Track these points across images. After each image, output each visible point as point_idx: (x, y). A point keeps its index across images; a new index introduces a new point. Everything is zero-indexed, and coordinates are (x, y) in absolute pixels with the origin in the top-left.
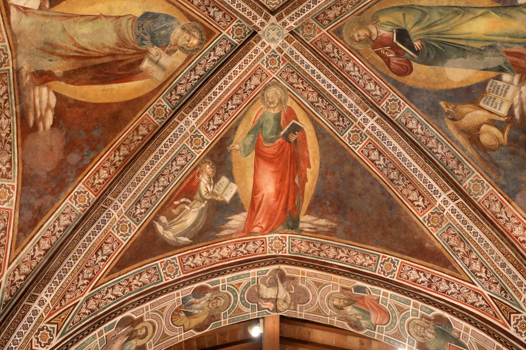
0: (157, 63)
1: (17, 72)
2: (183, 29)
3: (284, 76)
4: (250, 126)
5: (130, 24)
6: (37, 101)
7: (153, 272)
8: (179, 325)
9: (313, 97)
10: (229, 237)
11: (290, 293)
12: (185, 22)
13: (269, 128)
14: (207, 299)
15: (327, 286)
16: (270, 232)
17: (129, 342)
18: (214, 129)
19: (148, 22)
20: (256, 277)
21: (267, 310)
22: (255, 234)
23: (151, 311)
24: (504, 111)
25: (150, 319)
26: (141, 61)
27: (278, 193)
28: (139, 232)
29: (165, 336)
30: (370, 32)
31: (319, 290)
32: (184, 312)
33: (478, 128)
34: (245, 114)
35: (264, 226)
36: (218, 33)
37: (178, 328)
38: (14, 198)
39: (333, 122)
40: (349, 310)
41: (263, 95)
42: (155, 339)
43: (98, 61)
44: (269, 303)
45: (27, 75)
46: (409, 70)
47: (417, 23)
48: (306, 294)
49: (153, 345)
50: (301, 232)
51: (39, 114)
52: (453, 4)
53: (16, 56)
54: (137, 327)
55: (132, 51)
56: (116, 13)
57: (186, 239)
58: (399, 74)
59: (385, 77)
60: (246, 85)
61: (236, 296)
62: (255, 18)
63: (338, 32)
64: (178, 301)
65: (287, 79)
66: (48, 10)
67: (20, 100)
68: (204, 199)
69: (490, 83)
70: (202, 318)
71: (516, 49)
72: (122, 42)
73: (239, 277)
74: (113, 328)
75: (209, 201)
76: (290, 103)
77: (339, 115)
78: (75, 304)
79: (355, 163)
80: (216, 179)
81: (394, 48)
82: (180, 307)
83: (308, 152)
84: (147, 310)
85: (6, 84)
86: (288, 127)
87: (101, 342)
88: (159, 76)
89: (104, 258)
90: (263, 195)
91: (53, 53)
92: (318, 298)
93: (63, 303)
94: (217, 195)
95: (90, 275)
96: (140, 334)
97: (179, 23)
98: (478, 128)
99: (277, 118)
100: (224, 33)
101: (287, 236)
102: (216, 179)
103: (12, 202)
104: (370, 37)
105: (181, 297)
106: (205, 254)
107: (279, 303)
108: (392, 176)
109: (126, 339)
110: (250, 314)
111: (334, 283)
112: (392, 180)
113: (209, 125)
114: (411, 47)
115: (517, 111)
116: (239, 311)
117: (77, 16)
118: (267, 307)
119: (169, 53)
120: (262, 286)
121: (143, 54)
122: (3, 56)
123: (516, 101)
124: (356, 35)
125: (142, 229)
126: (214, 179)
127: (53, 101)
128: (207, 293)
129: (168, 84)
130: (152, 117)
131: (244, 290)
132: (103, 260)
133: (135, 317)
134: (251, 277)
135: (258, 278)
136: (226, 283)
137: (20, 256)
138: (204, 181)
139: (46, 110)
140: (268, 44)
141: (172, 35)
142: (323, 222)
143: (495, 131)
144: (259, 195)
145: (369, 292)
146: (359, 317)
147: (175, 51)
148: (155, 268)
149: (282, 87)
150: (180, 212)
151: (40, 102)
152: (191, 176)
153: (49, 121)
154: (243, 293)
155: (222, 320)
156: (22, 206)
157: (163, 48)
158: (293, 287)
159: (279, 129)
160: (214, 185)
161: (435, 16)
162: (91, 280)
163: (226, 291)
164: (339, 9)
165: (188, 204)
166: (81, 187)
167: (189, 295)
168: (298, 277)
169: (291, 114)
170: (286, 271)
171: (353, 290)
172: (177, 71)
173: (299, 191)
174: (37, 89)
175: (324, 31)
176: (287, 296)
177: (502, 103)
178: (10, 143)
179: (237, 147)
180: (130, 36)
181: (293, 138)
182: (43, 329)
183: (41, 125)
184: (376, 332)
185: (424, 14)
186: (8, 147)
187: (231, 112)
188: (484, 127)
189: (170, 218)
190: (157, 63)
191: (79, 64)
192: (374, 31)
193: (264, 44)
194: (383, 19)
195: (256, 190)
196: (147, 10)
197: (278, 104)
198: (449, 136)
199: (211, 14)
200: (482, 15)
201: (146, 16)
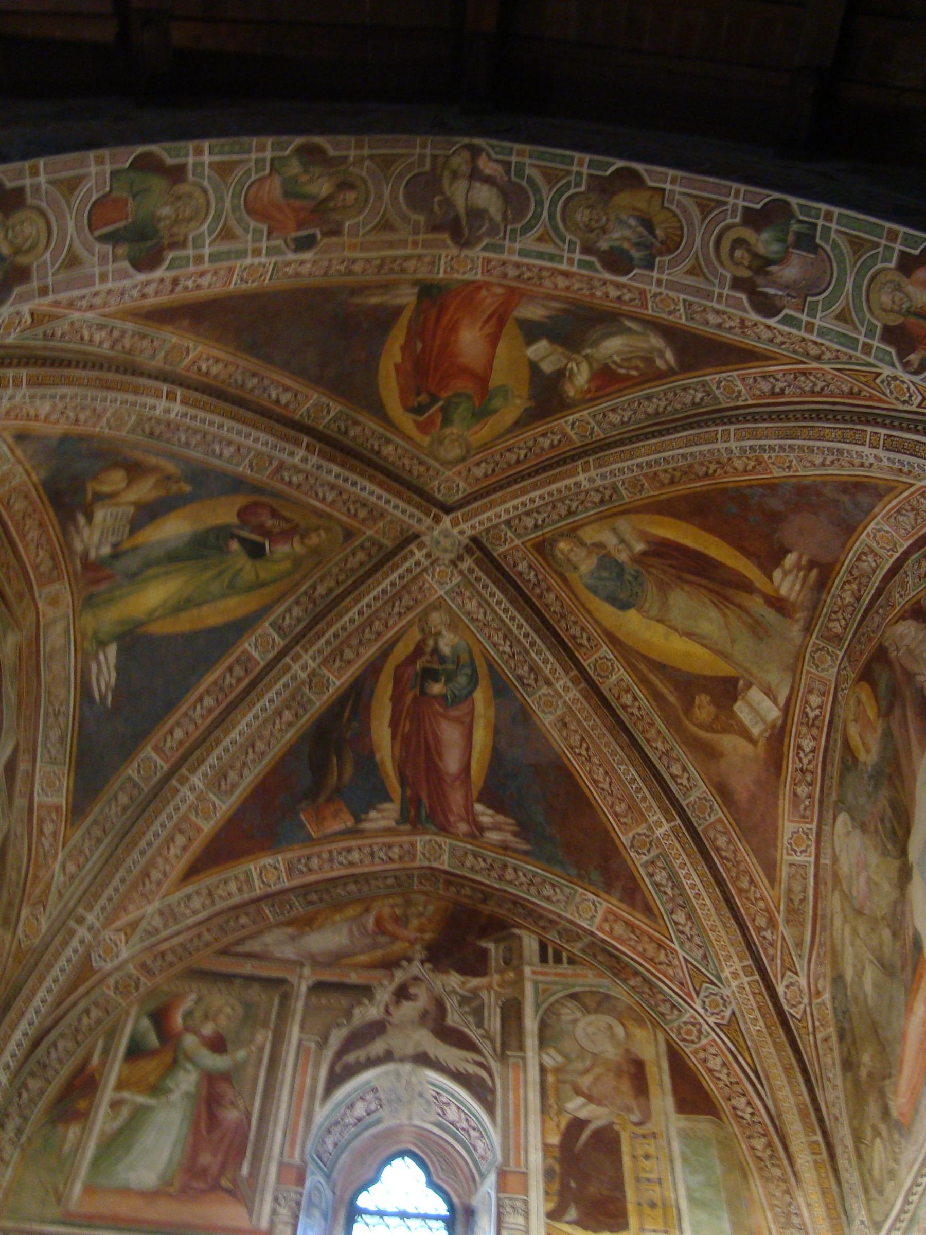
0: (622, 541)
1: (808, 630)
2: (576, 568)
3: (431, 472)
4: (492, 420)
5: (647, 605)
6: (797, 587)
7: (697, 317)
8: (670, 215)
9: (388, 450)
10: (548, 297)
11: (443, 193)
12: (572, 576)
13: (461, 411)
14: (606, 237)
15: (369, 227)
16: (473, 282)
17: (771, 256)
18: (553, 433)
19: (623, 596)
20: (507, 243)
21: (494, 156)
22: (500, 285)
23: (714, 285)
24: (100, 515)
25: (720, 270)
26: (644, 554)
27: (454, 328)
28: (707, 371)
29: (705, 207)
30: (302, 542)
31: (384, 215)
32: (655, 237)
33: (130, 483)
34: (500, 437)
35: (484, 292)
36: (528, 544)
37: (674, 208)
38: (872, 525)
39: (356, 423)
40: (323, 188)
41: (468, 451)
42: (721, 216)
43: (704, 582)
44: (487, 171)
45: (798, 621)
46: (243, 514)
47: (241, 569)
48: (411, 199)
49: (729, 207)
50: (415, 283)
51: (801, 574)
52: (195, 611)
53: (801, 647)
54: (746, 273)
55: (654, 571)
56: (660, 628)
57: (628, 323)
58: (256, 505)
59: (277, 495)
60: (494, 470)
61: (552, 216)
62: (471, 571)
63: (349, 534)
64: (661, 270)
65: (428, 469)
66: (743, 677)
67: (817, 604)
68: (587, 357)
69: (125, 536)
70: (624, 199)
71: (103, 587)
72: (664, 588)
73: (540, 255)
74: (786, 315)
75: (579, 352)
76: (425, 441)
77: (346, 432)
78: (838, 370)
79: (317, 381)
80: (561, 375)
81: (267, 533)
82: (661, 254)
83: (399, 383)
84: (720, 296)
85: (826, 627)
86: (431, 411)
87: (812, 313)
88: (624, 525)
89: (772, 380)
90: (481, 329)
91: (757, 621)
92: (387, 193)
93: (856, 390)
94: (563, 354)
95: (802, 378)
96: (746, 255)
97: (581, 577)
98: (130, 483)
99: (447, 421)
100: (518, 542)
101: (441, 275)
102: (561, 375)
103: (877, 524)
104: (303, 537)
105: (655, 274)
106: (599, 294)
107: (465, 169)
108: (255, 381)
109: (773, 268)
110: (527, 161)
111: (354, 240)
112: (254, 375)
113: (560, 441)
114: (243, 541)
115: (81, 520)
116: (551, 177)
117: (710, 649)
118: (492, 164)
119: (600, 545)
120: (498, 218)
121: (639, 559)
122: (816, 656)
123: (86, 533)
124: (323, 535)
125: (700, 373)
126: (564, 375)
127: (777, 574)
128: (604, 252)
129: (611, 512)
130: (646, 485)
131: (533, 222)
132: (777, 380)
133: (743, 297)
134: (517, 246)
135: (504, 238)
136: (566, 255)
137: (893, 478)
138: (582, 377)
139: (790, 571)
140: (455, 531)
141: (593, 566)
142: (374, 300)
143: (105, 489)
144: (488, 329)
145: (287, 246)
146: (304, 178)
147: (594, 545)
148: (693, 319)
149: (436, 459)
150: (628, 359)
151: (794, 584)
152: (601, 393)
153: (790, 560)
154: (537, 216)
155: (585, 170)
156: (868, 512)
157: (608, 555)
158: (436, 208)
159: (445, 410)
160: (565, 368)
161: (215, 587)
162: (804, 373)
163: (569, 237)
164: (349, 566)
165: (615, 362)
166: (777, 473)
167: (640, 267)
168: (426, 232)
169: (423, 428)
170: (449, 242)
171: (319, 236)
172: (596, 521)
173: (416, 332)
174: (793, 597)
175: (369, 533)
176: (451, 185)
177: (105, 520)
178: (850, 572)
179: (518, 402)
180: (651, 592)
181: (423, 398)
182: (897, 399)
183: (804, 562)
184: (268, 155)
185: (231, 586)
186: (855, 572)
187: (522, 444)
188: (123, 485)
189: (649, 360)
190: (622, 541)
191: (730, 592)
192: (298, 547)
193: (462, 532)
194: (287, 565)
195: (494, 340)
196: (620, 613)
197: (445, 438)
198: (172, 457)
199: (533, 573)
200: (154, 610)
201: (624, 606)
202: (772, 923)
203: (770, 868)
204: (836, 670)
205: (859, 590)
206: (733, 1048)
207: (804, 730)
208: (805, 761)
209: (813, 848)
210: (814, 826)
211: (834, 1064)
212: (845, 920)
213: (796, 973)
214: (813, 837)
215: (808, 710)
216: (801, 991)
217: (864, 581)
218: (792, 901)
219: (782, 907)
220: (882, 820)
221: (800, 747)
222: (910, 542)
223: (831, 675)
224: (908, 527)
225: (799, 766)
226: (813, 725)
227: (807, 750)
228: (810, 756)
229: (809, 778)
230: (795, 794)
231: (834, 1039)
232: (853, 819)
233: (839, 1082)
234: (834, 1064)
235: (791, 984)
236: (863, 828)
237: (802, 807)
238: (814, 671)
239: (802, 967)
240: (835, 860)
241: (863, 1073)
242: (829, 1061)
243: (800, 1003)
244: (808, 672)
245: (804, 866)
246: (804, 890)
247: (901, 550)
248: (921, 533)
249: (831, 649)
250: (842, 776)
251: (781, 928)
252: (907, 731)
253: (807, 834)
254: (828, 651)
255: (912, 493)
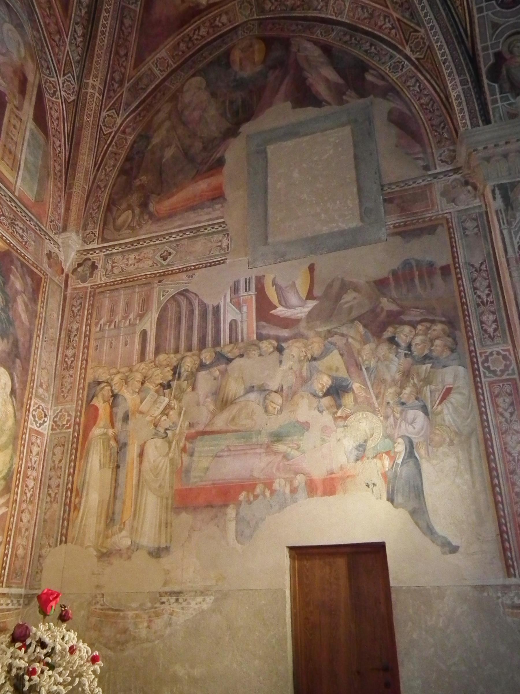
202: (121, 83)
203: (139, 60)
204: (246, 20)
205: (298, 7)
206: (65, 116)
207: (208, 24)
208: (195, 37)
209: (165, 74)
210: (174, 66)
211: (114, 166)
212: (169, 118)
213: (118, 115)
214: (170, 70)
215: (218, 19)
216: (115, 124)
217: (306, 6)
218: (138, 84)
219: (132, 81)
220: (232, 103)
221: (199, 28)
222: (347, 21)
223: (241, 19)
224: (356, 16)
225: (191, 35)
226: (213, 27)
227: (201, 34)
228: (199, 38)
229: (190, 45)
230: (178, 44)
231: (122, 157)
232: (208, 85)
233: (114, 175)
234: (114, 166)
235: (112, 116)
236: (213, 95)
237: (176, 53)
238: (237, 8)
239: (122, 115)
240: (180, 90)
241: (137, 182)
242: (112, 162)
243: (110, 128)
244: (234, 5)
245: (155, 77)
246: (147, 86)
247: (339, 19)
248: (358, 25)
249: (254, 10)
250: (211, 63)
251: (124, 89)
252: (281, 83)
253: (168, 66)
254: (251, 9)
255: (383, 11)
